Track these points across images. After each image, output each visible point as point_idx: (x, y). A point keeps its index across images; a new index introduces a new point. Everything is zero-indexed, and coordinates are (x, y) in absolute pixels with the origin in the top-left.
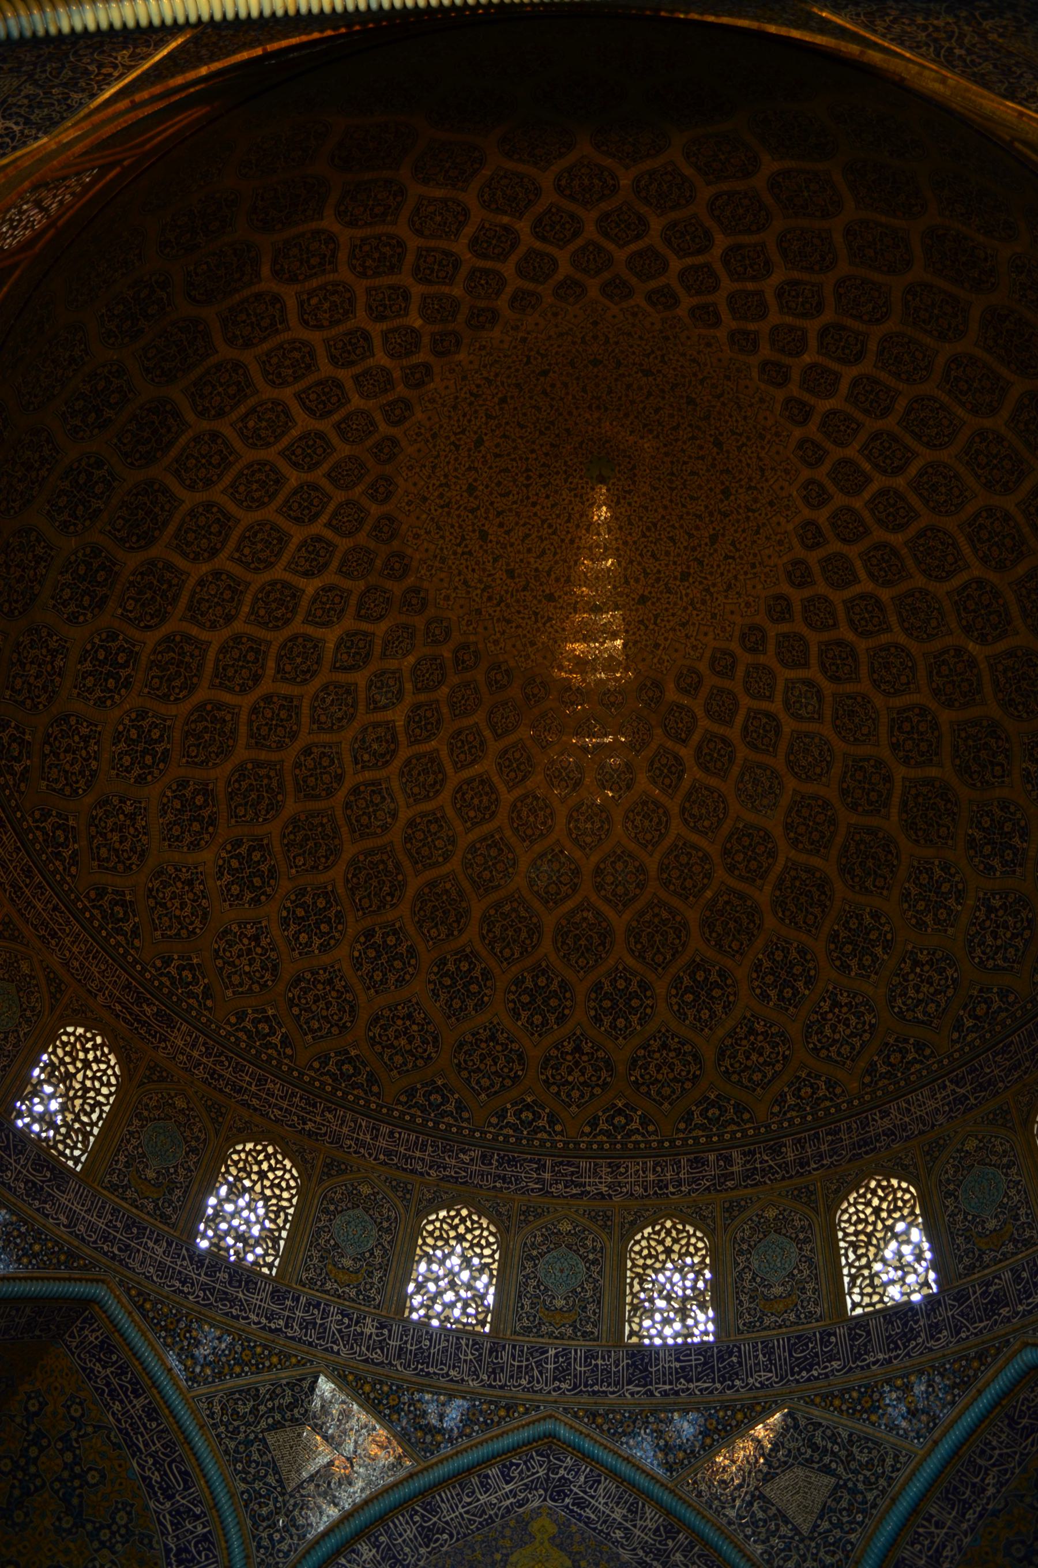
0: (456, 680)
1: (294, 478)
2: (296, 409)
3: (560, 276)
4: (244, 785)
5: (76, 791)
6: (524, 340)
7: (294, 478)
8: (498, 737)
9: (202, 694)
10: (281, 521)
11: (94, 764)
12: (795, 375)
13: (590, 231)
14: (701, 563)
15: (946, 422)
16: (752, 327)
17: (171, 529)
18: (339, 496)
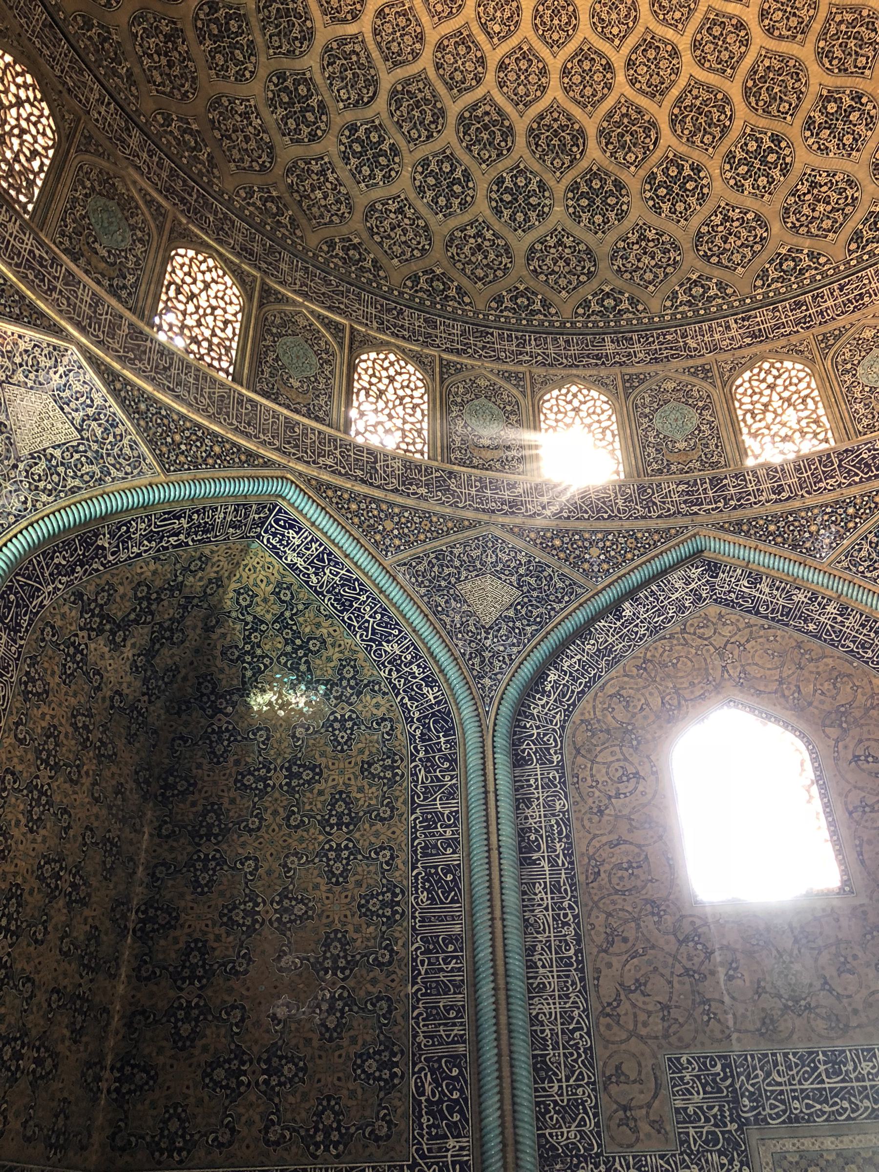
4: (838, 53)
5: (762, 239)
9: (735, 90)
11: (750, 216)
17: (576, 112)
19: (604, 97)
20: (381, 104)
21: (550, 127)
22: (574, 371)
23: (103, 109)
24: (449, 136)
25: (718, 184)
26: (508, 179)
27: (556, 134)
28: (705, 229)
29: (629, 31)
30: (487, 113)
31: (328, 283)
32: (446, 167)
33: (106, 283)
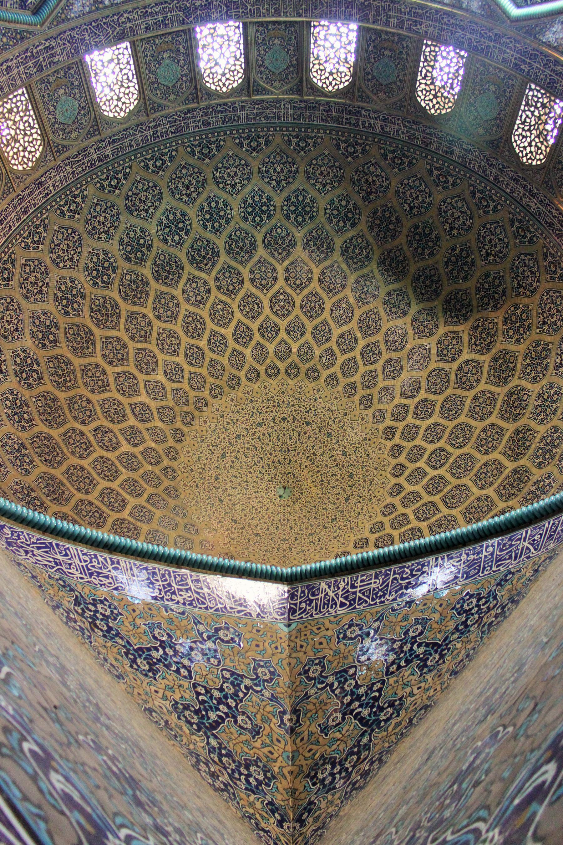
0: (158, 472)
1: (203, 343)
2: (234, 324)
3: (352, 380)
4: (63, 365)
6: (316, 399)
7: (203, 343)
8: (148, 501)
9: (97, 332)
10: (183, 347)
12: (407, 473)
13: (379, 365)
14: (297, 539)
15: (464, 496)
16: (404, 444)
18: (204, 371)
19: (154, 302)
20: (259, 238)
21: (174, 274)
22: (124, 126)
23: (396, 127)
24: (220, 242)
25: (83, 279)
26: (184, 236)
27: (169, 273)
28: (79, 250)
29: (158, 338)
30: (206, 265)
31: (267, 117)
32: (216, 225)
33: (384, 36)
